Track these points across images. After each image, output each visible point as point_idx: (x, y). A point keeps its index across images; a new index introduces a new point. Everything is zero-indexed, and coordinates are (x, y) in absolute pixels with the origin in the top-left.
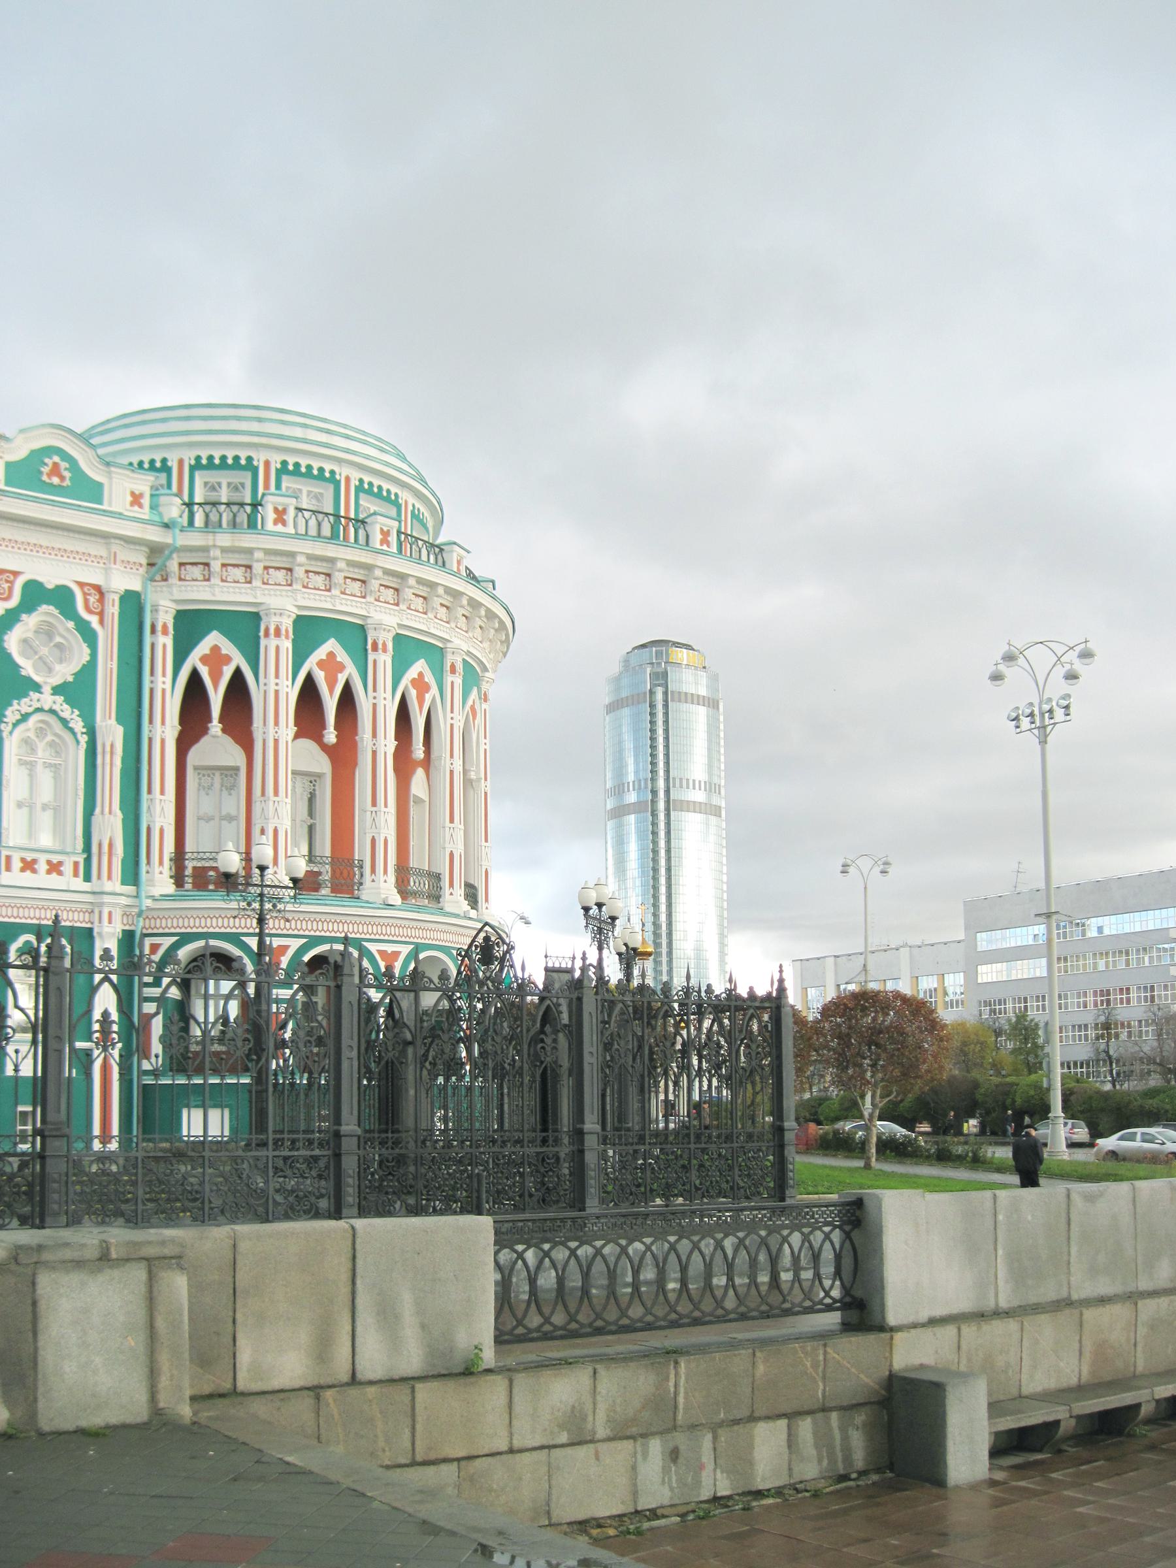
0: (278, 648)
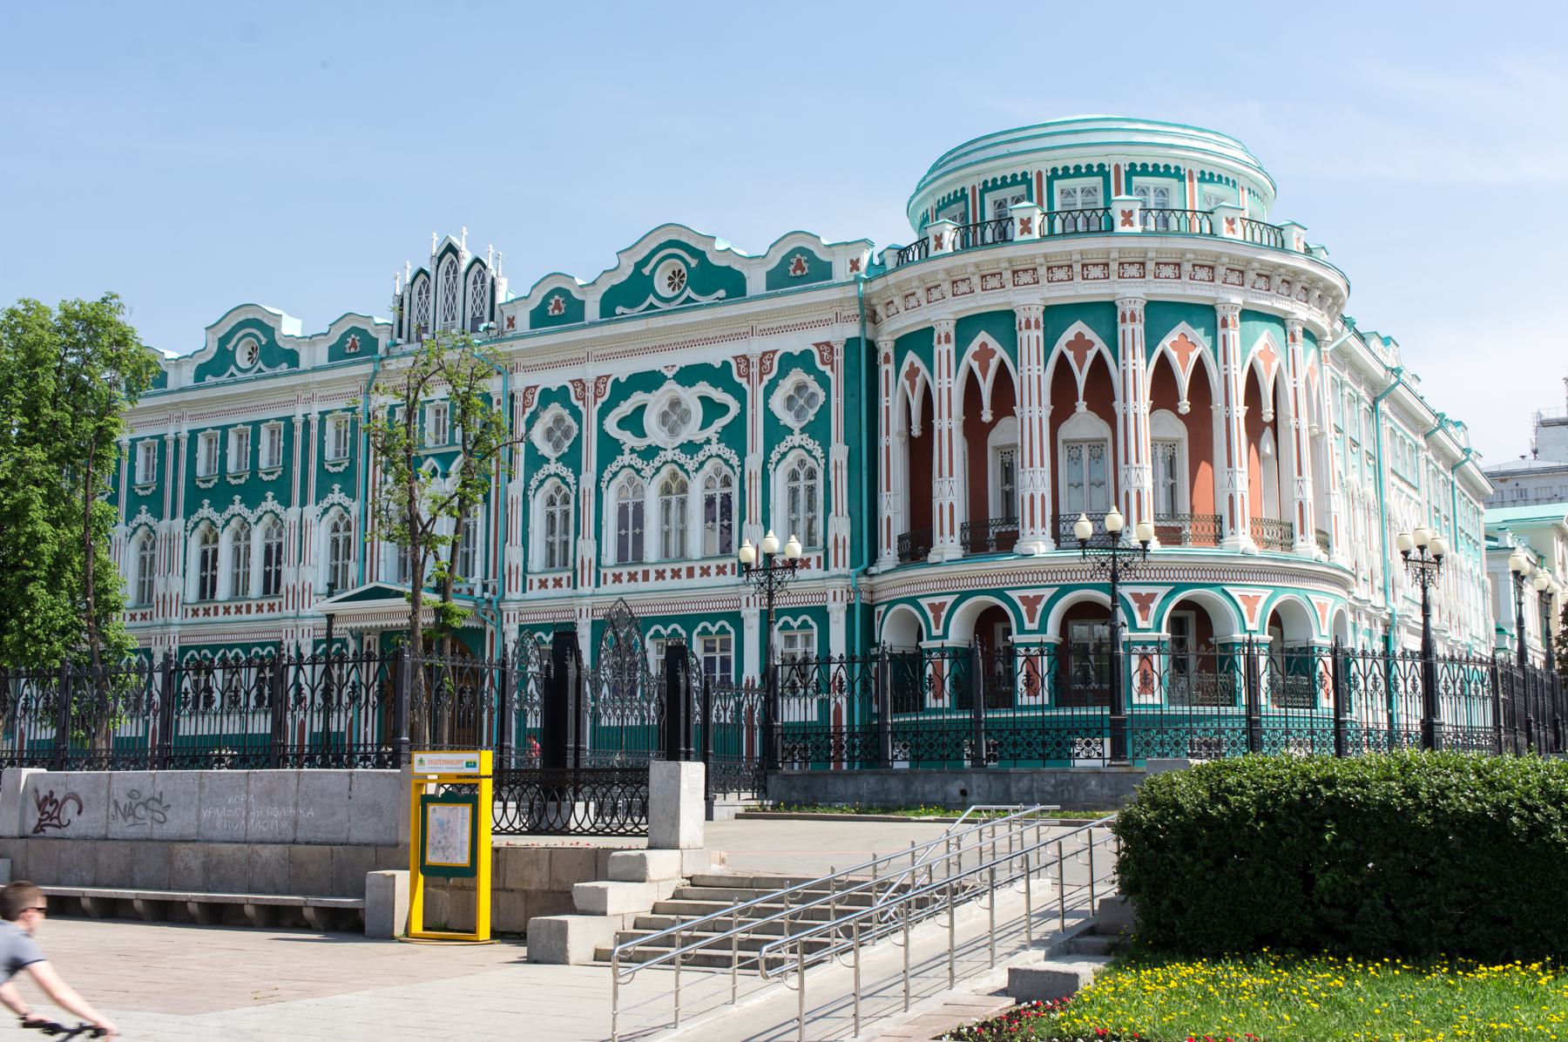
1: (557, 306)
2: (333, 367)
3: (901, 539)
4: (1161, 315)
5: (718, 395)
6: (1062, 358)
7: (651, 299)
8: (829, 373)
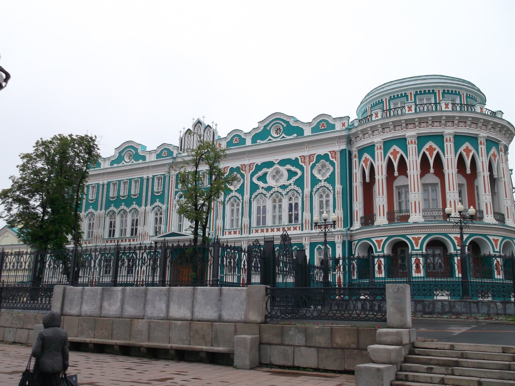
0: (449, 146)
1: (236, 140)
2: (158, 161)
3: (361, 218)
4: (459, 139)
5: (293, 169)
6: (424, 154)
7: (270, 137)
8: (334, 161)
